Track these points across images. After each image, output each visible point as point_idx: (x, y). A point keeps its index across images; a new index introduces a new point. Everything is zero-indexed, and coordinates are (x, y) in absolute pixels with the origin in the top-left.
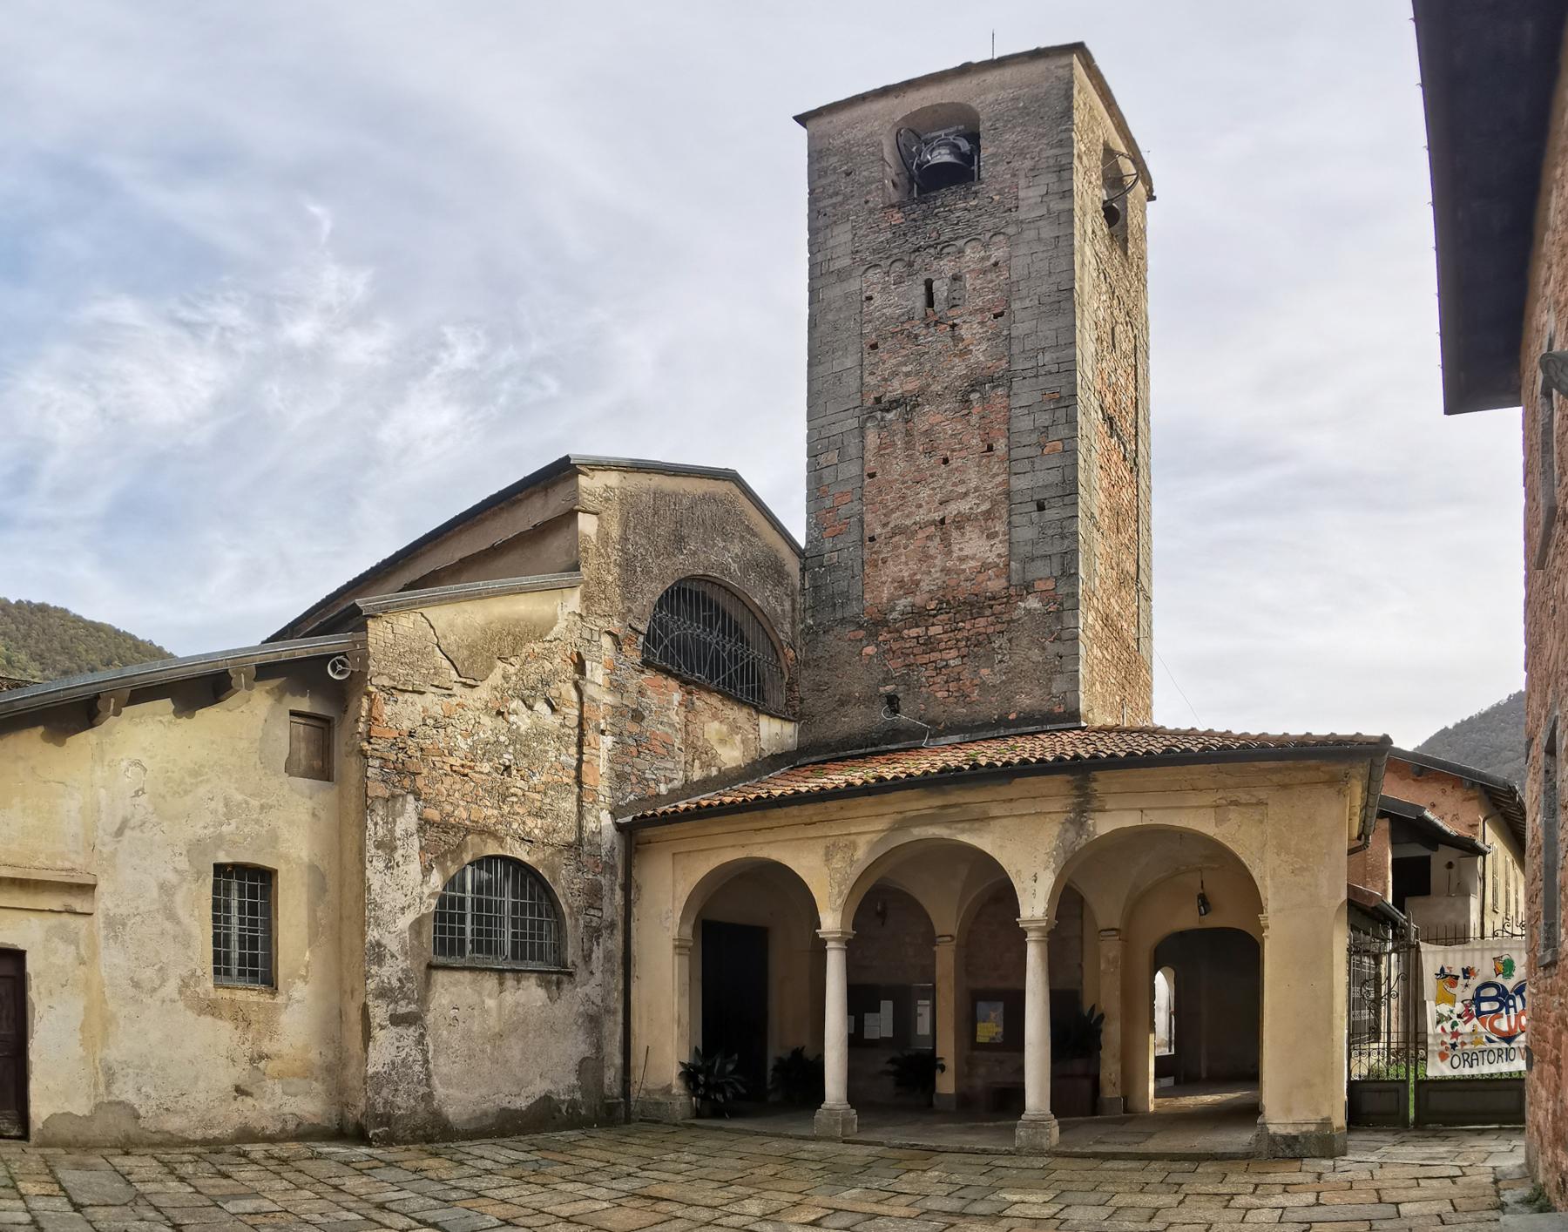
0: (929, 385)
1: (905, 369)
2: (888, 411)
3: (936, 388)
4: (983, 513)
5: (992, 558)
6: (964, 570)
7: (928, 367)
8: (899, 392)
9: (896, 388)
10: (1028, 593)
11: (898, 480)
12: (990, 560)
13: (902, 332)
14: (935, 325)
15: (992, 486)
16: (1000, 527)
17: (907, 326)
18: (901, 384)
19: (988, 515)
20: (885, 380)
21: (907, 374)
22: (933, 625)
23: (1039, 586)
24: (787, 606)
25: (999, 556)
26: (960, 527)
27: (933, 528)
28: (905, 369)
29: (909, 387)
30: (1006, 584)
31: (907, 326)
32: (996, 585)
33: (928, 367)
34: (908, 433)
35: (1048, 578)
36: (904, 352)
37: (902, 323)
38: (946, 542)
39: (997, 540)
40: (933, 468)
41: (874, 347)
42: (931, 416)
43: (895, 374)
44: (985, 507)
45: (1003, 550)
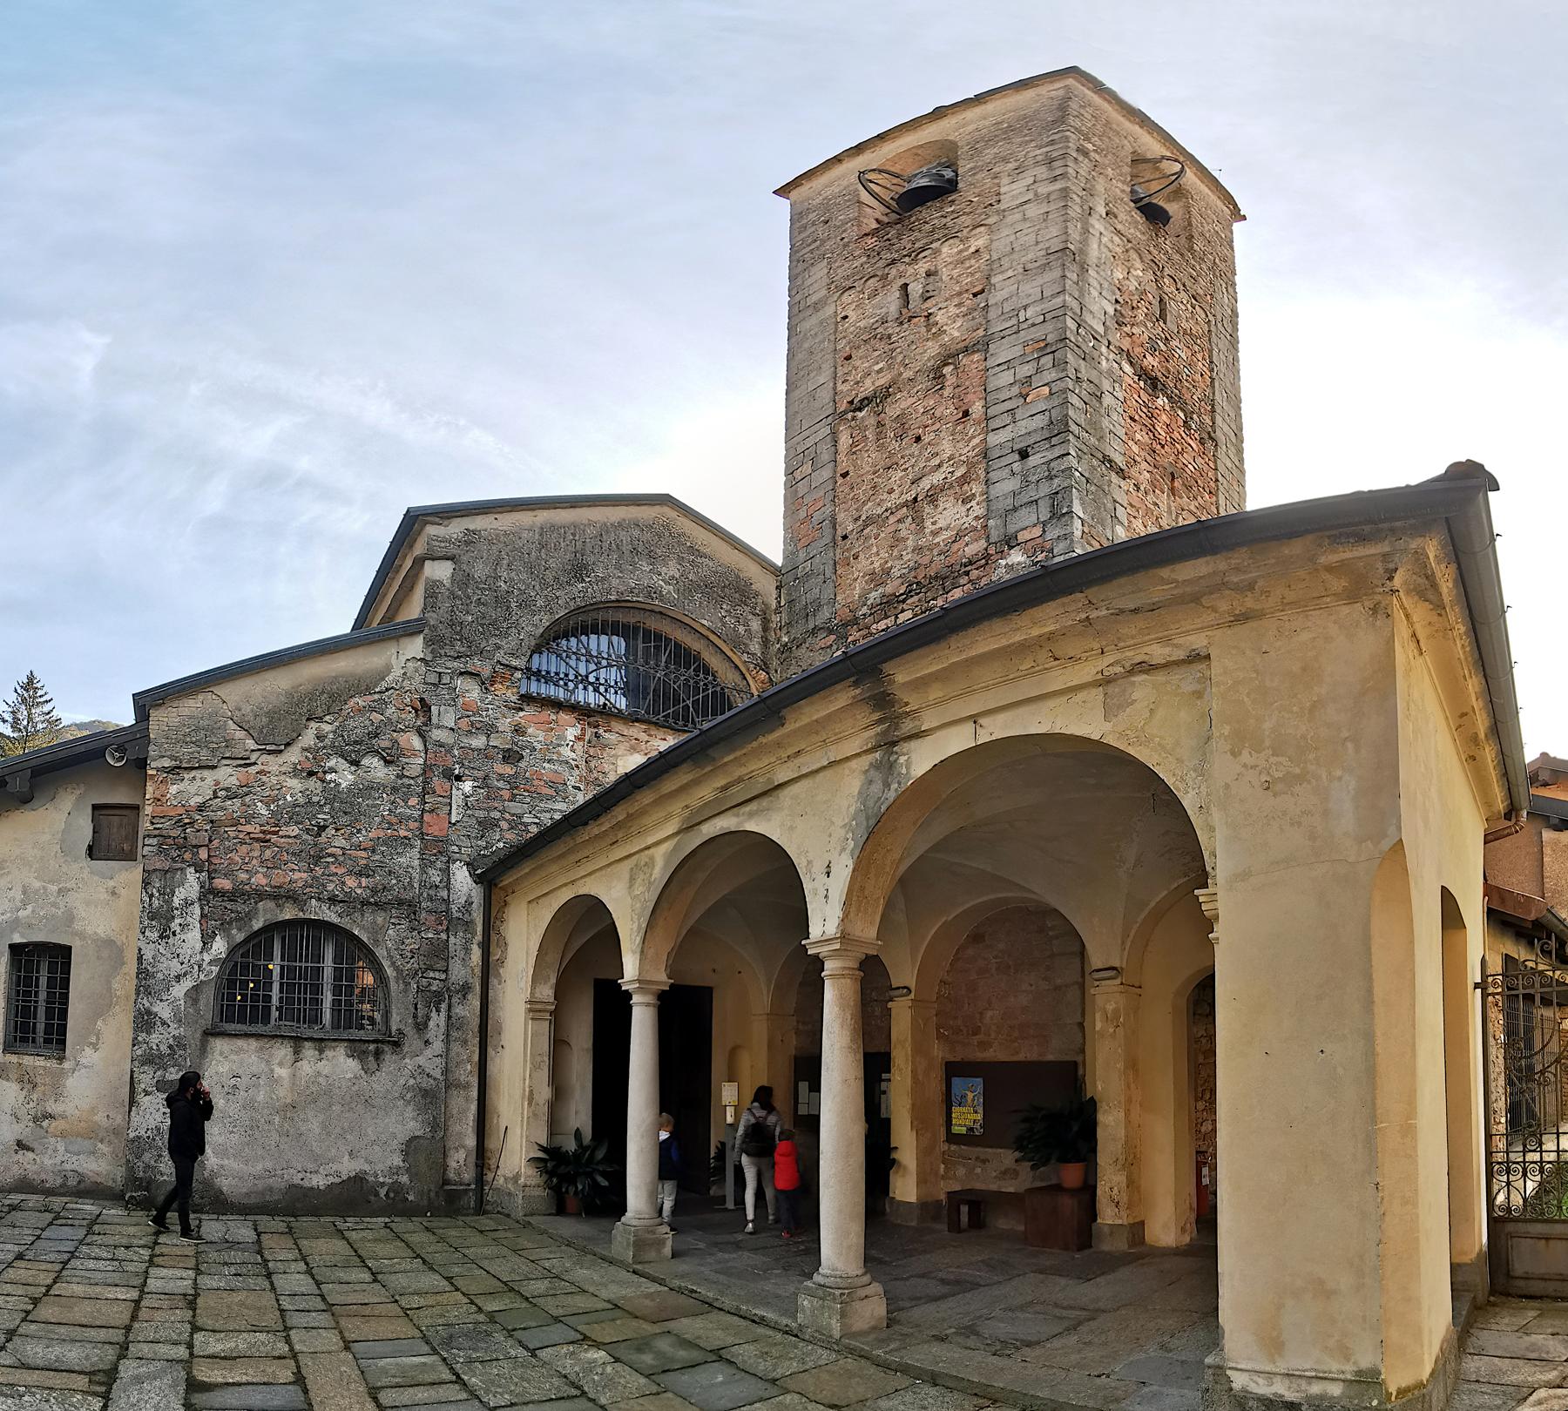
0: (900, 374)
3: (908, 374)
10: (1011, 548)
22: (903, 611)
23: (1022, 537)
24: (756, 625)
32: (974, 548)
33: (900, 358)
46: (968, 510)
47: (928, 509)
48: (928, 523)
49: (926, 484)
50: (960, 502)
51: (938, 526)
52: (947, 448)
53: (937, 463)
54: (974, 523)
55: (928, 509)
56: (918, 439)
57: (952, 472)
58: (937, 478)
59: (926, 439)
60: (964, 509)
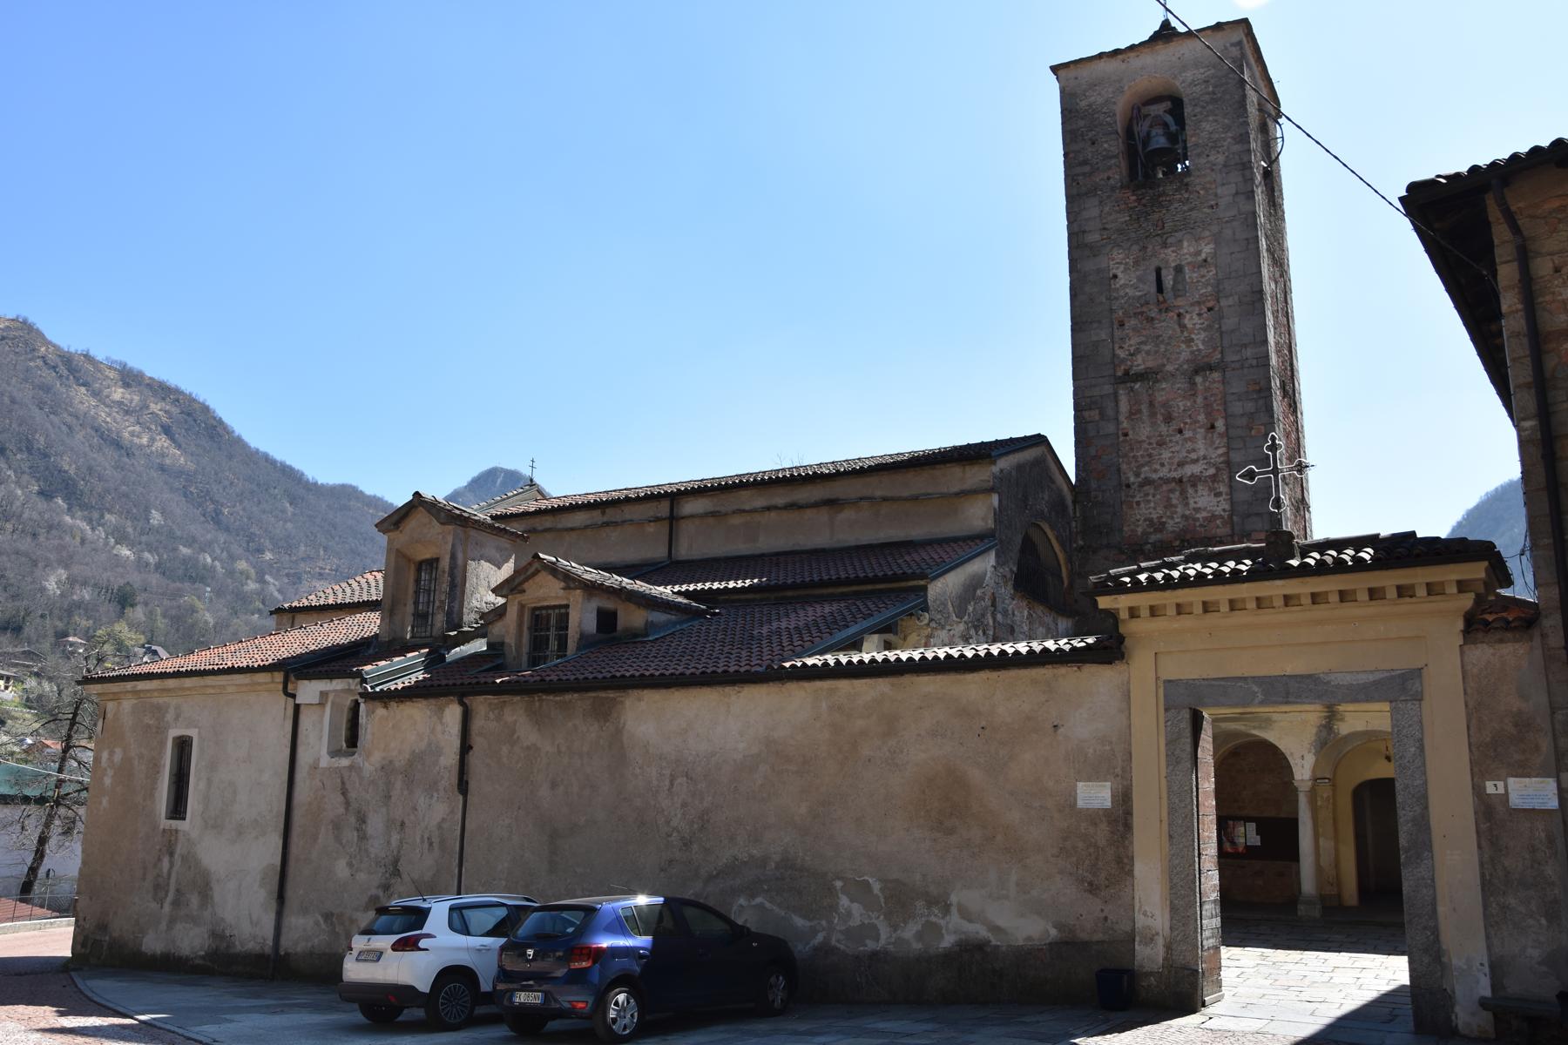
0: (1164, 365)
1: (1147, 348)
2: (1135, 381)
3: (1169, 368)
4: (1210, 476)
5: (1218, 511)
6: (1198, 518)
7: (1162, 348)
8: (1142, 367)
9: (1140, 363)
11: (1145, 441)
12: (1217, 513)
13: (1142, 313)
14: (1166, 312)
15: (1217, 454)
16: (1223, 488)
17: (1144, 309)
18: (1144, 361)
19: (1214, 478)
20: (1132, 355)
21: (1148, 353)
25: (1224, 510)
26: (1194, 485)
27: (1174, 484)
28: (1147, 348)
29: (1150, 364)
30: (1230, 532)
31: (1144, 309)
34: (1151, 404)
35: (1261, 531)
36: (1144, 333)
37: (1142, 306)
38: (1183, 492)
39: (1221, 498)
40: (1172, 435)
41: (1122, 325)
42: (1165, 391)
43: (1138, 351)
44: (1212, 471)
45: (1227, 507)
46: (1218, 502)
47: (1190, 491)
48: (1191, 501)
49: (1189, 470)
50: (1212, 494)
51: (1198, 506)
52: (1201, 448)
53: (1195, 457)
54: (1222, 513)
55: (1190, 491)
56: (1180, 431)
57: (1206, 469)
58: (1195, 469)
59: (1188, 434)
60: (1215, 500)
